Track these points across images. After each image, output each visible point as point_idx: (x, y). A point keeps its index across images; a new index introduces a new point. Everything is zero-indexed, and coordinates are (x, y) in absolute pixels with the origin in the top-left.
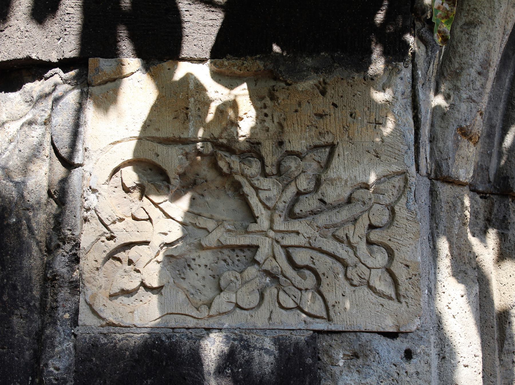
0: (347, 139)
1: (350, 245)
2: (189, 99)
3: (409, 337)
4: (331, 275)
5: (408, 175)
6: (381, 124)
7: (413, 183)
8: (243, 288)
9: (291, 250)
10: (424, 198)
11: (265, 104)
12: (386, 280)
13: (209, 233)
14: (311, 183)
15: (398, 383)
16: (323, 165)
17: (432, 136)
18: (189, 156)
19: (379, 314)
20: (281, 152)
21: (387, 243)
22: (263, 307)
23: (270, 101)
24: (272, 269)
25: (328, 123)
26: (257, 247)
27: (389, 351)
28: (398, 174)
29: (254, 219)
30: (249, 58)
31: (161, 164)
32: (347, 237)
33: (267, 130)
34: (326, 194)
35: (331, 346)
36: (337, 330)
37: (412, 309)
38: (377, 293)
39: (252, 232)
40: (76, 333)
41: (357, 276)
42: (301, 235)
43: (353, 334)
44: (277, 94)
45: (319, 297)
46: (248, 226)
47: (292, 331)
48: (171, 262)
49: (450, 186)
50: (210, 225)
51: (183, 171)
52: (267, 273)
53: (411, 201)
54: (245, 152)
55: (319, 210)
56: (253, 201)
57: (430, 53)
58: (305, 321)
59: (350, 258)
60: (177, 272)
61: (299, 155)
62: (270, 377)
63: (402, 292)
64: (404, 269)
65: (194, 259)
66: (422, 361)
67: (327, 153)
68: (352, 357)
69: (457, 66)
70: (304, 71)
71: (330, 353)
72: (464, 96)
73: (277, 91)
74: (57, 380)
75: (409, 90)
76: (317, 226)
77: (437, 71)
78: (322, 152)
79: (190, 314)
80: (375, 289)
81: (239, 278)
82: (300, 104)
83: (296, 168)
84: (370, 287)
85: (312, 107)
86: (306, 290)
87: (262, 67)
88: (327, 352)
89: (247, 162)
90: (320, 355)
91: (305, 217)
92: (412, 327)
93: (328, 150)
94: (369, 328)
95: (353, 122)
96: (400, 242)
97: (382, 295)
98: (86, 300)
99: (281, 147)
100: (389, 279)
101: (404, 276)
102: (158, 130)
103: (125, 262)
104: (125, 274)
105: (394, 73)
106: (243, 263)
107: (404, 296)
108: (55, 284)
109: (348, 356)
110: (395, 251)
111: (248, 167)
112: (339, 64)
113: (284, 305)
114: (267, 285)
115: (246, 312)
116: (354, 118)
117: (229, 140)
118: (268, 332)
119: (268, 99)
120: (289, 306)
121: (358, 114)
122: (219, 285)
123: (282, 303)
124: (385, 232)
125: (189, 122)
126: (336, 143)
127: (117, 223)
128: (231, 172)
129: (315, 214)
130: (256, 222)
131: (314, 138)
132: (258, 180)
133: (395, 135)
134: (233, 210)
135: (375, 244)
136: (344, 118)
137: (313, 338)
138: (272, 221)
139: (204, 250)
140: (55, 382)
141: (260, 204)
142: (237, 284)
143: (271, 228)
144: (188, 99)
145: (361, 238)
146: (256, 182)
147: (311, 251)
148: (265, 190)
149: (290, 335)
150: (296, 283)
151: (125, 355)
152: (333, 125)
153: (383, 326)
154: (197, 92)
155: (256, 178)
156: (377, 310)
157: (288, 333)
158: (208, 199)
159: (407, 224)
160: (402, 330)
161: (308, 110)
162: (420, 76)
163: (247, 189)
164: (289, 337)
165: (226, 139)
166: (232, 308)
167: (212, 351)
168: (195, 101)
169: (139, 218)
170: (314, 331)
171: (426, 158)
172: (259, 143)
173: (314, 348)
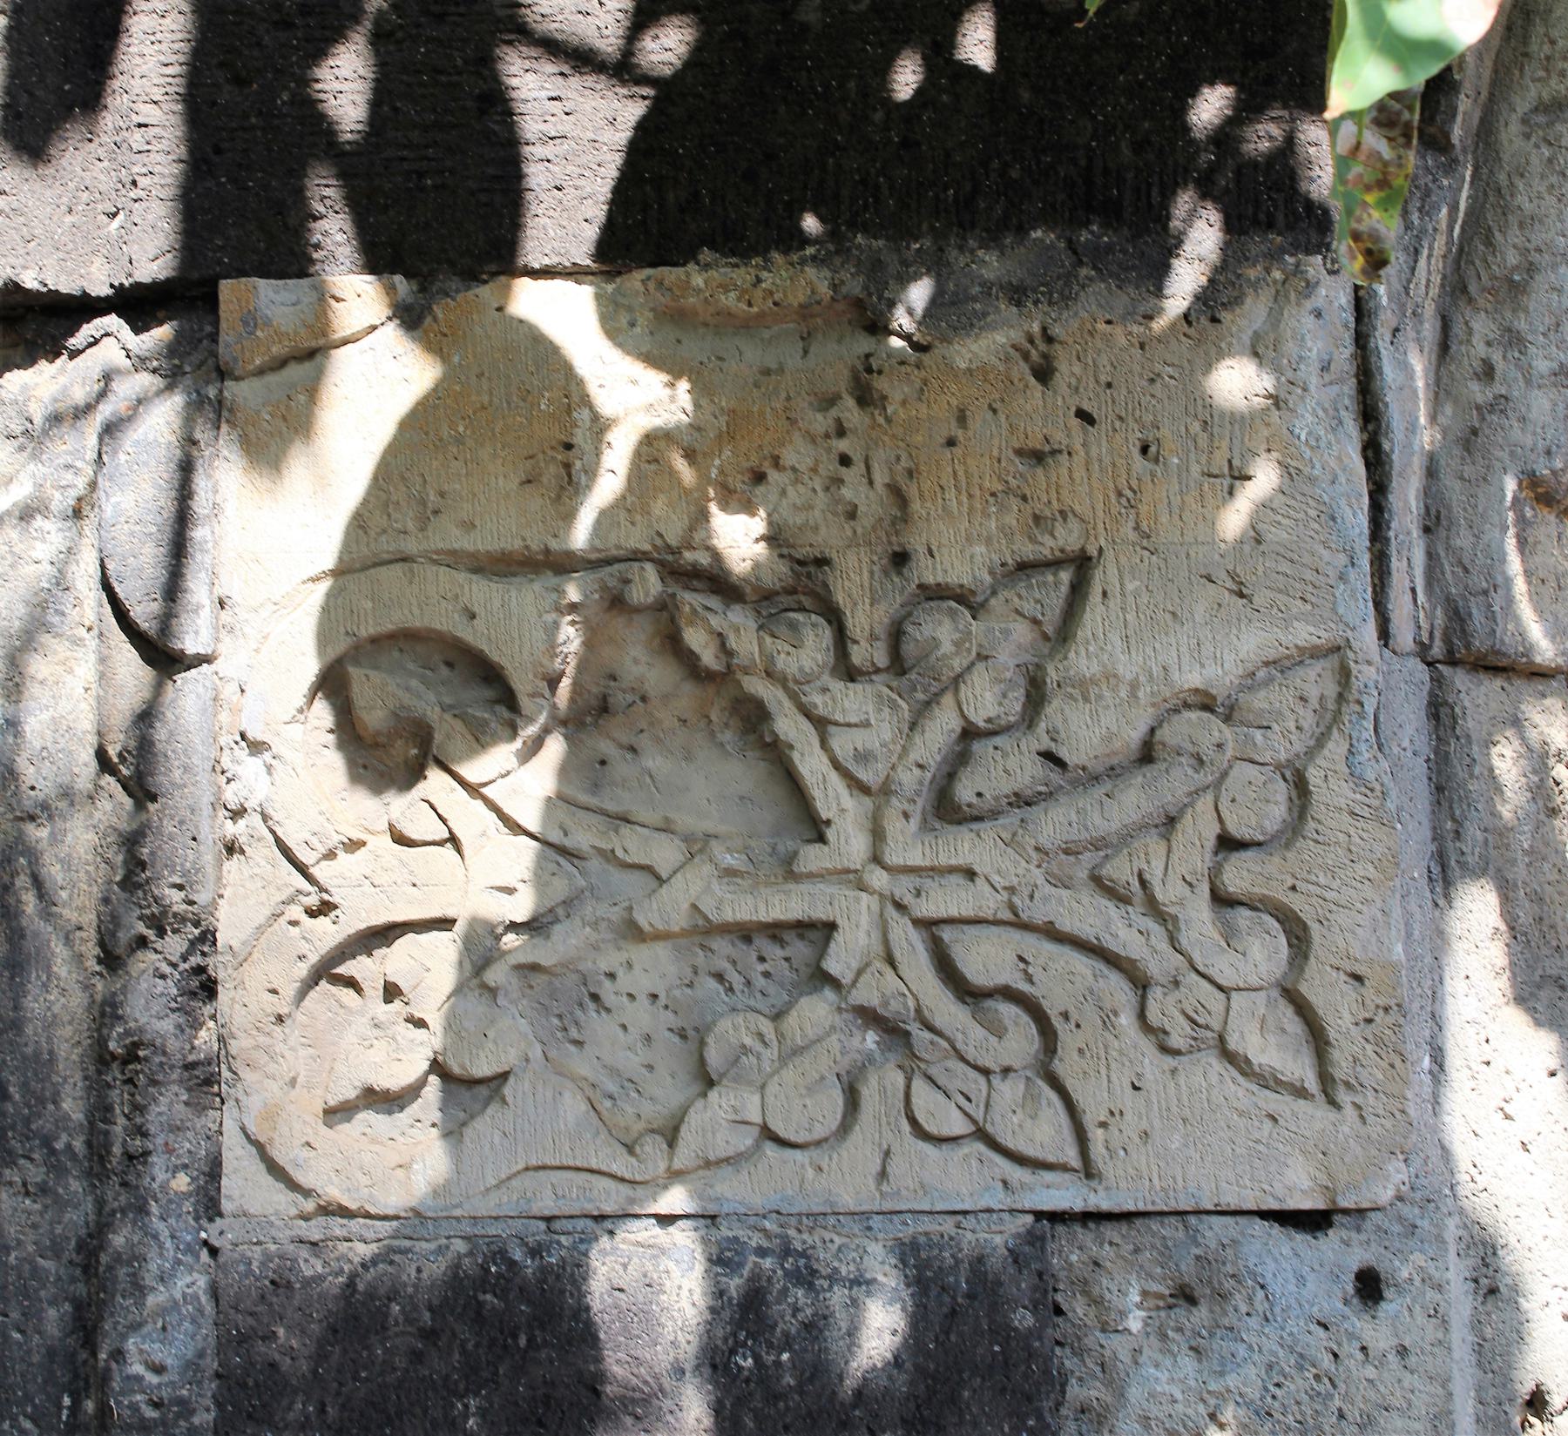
0: (1133, 536)
1: (1154, 908)
2: (575, 414)
3: (1368, 1225)
4: (1091, 1018)
5: (1350, 654)
7: (1371, 684)
8: (784, 1072)
9: (947, 934)
10: (1409, 730)
11: (839, 421)
12: (1283, 1030)
14: (1010, 695)
15: (1334, 1386)
16: (1049, 629)
17: (1433, 512)
19: (1261, 1148)
20: (904, 587)
21: (1285, 900)
22: (856, 1135)
23: (856, 411)
24: (886, 1004)
25: (1061, 482)
26: (831, 927)
27: (1306, 1274)
28: (1316, 653)
29: (817, 829)
30: (777, 257)
31: (485, 648)
32: (1143, 883)
33: (852, 515)
34: (1063, 735)
35: (1096, 1264)
36: (1116, 1209)
37: (1374, 1129)
38: (1255, 1074)
42: (980, 881)
43: (1173, 1219)
44: (881, 384)
45: (1053, 1096)
46: (796, 853)
47: (960, 1218)
48: (531, 987)
49: (1498, 682)
50: (664, 854)
52: (869, 1017)
53: (1363, 747)
55: (1043, 789)
56: (811, 765)
57: (1415, 217)
58: (1005, 1183)
60: (556, 1021)
61: (965, 599)
62: (890, 1377)
63: (1341, 1067)
64: (1345, 987)
65: (611, 976)
66: (1417, 1309)
67: (1064, 589)
69: (1512, 258)
70: (975, 299)
71: (1096, 1291)
72: (1542, 366)
73: (880, 372)
74: (157, 1405)
75: (1345, 353)
76: (1037, 849)
77: (1444, 277)
78: (1045, 583)
79: (604, 1168)
80: (1248, 1061)
81: (770, 1035)
82: (962, 419)
83: (957, 644)
84: (1229, 1056)
85: (1005, 425)
86: (1007, 1071)
87: (824, 289)
88: (1084, 1287)
89: (782, 630)
90: (1059, 1298)
91: (995, 814)
92: (1380, 1191)
93: (1065, 576)
94: (1231, 1200)
95: (1153, 475)
96: (1330, 895)
97: (1272, 1083)
98: (243, 1129)
99: (900, 573)
100: (1294, 1026)
101: (1346, 1015)
102: (469, 526)
103: (374, 991)
104: (377, 1032)
105: (1293, 295)
106: (782, 985)
107: (1347, 1084)
108: (137, 1072)
109: (1160, 1296)
110: (1314, 927)
111: (787, 648)
112: (1095, 268)
113: (932, 1128)
114: (870, 1059)
115: (798, 1155)
116: (1157, 461)
118: (876, 1222)
119: (850, 402)
120: (946, 1132)
121: (1168, 445)
122: (702, 1061)
124: (1276, 859)
126: (1092, 551)
127: (341, 854)
128: (729, 666)
129: (1028, 804)
130: (821, 839)
131: (1018, 537)
132: (825, 690)
133: (1301, 516)
134: (742, 798)
135: (1242, 904)
136: (1121, 462)
137: (1034, 1239)
138: (878, 834)
139: (644, 941)
140: (150, 1413)
141: (834, 776)
142: (764, 1057)
143: (876, 859)
144: (569, 411)
145: (1190, 885)
146: (817, 699)
147: (1016, 935)
148: (849, 725)
149: (953, 1232)
151: (386, 1315)
152: (1083, 489)
153: (1279, 1189)
155: (819, 683)
156: (1257, 1135)
157: (948, 1226)
158: (654, 761)
159: (1352, 831)
161: (990, 439)
162: (1384, 301)
163: (789, 725)
164: (951, 1238)
166: (749, 1142)
167: (685, 1293)
169: (414, 836)
170: (1039, 1215)
171: (1413, 590)
172: (822, 562)
173: (1040, 1275)
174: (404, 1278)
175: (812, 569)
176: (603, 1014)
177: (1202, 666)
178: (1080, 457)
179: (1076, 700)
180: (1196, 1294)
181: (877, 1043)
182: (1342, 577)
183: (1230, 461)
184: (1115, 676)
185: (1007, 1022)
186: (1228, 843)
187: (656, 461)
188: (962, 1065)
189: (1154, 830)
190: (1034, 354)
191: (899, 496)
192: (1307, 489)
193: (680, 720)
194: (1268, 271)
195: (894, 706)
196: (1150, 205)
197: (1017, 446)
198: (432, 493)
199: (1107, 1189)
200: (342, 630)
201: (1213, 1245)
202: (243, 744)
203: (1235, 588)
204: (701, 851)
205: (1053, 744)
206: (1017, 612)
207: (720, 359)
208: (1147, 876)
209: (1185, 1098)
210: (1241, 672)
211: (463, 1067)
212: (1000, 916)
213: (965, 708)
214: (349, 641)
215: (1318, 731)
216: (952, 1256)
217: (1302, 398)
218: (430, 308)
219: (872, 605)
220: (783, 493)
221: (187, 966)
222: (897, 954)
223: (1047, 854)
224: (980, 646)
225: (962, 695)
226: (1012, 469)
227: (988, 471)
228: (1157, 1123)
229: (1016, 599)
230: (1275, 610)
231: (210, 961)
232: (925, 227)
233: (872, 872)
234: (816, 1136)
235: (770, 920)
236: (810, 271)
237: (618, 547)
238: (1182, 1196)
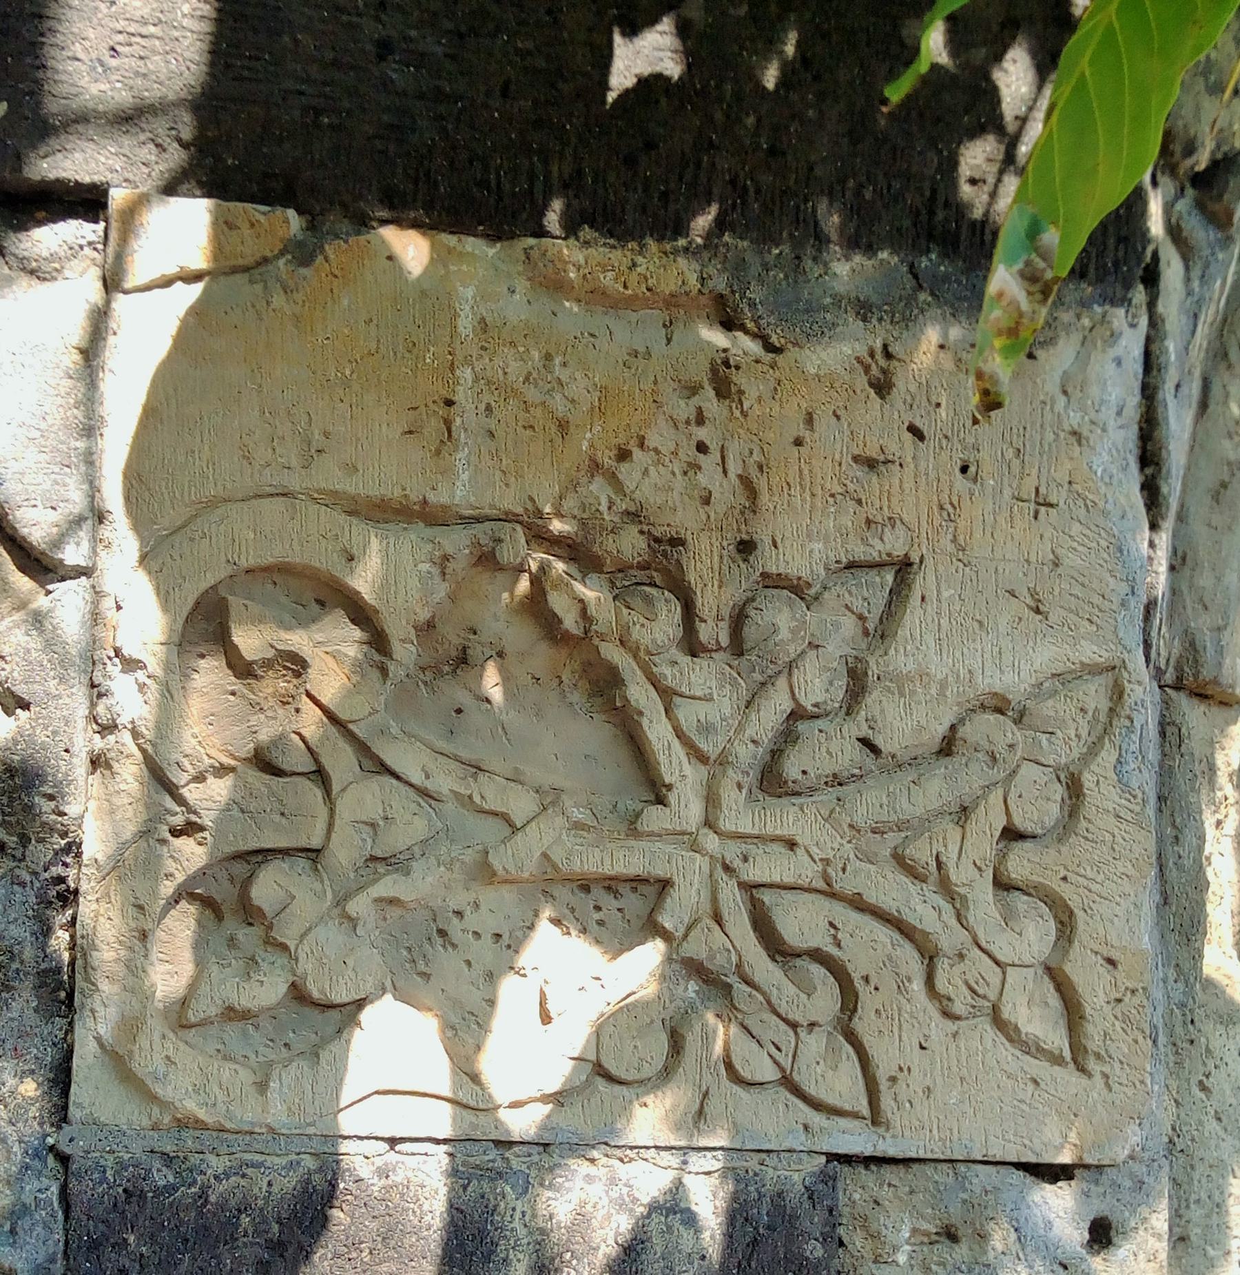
0: (950, 548)
1: (946, 887)
2: (458, 372)
4: (888, 982)
5: (1126, 675)
6: (1051, 505)
9: (767, 897)
11: (700, 411)
13: (515, 829)
14: (835, 682)
16: (871, 626)
18: (451, 566)
19: (1024, 1107)
21: (1057, 889)
23: (715, 400)
24: (712, 957)
26: (664, 885)
28: (1094, 670)
29: (658, 793)
33: (707, 501)
34: (880, 724)
36: (901, 1155)
39: (651, 834)
40: (68, 1151)
41: (964, 989)
42: (800, 851)
43: (945, 1166)
44: (739, 379)
46: (638, 815)
47: (764, 1156)
51: (428, 616)
52: (696, 969)
53: (1130, 758)
54: (631, 567)
55: (856, 771)
56: (657, 731)
57: (1196, 284)
58: (806, 1127)
59: (948, 936)
61: (797, 588)
63: (1094, 1041)
64: (1102, 970)
65: (459, 914)
66: (1141, 1256)
68: (935, 1238)
70: (826, 309)
71: (874, 1227)
73: (737, 368)
75: (1134, 401)
76: (851, 826)
82: (810, 420)
85: (847, 433)
88: (864, 1222)
89: (637, 602)
90: (841, 1231)
91: (812, 790)
92: (1119, 1150)
94: (997, 1153)
97: (1033, 1050)
100: (1054, 1000)
101: (1101, 993)
102: (351, 469)
105: (1099, 343)
107: (1098, 1056)
110: (1079, 913)
111: (642, 620)
112: (932, 294)
113: (746, 1074)
116: (975, 480)
117: (583, 523)
119: (711, 393)
120: (759, 1078)
121: (987, 468)
123: (738, 1067)
124: (1052, 852)
126: (915, 558)
127: (211, 780)
129: (840, 784)
130: (661, 801)
133: (1094, 545)
136: (944, 477)
137: (827, 1178)
138: (712, 800)
141: (676, 743)
143: (709, 823)
144: (452, 368)
145: (980, 869)
146: (667, 671)
149: (757, 1168)
150: (784, 1003)
152: (911, 500)
153: (1038, 1147)
154: (483, 348)
156: (1021, 1096)
159: (1116, 831)
160: (1089, 1160)
161: (832, 442)
162: (1173, 358)
163: (639, 693)
164: (756, 1174)
165: (575, 517)
167: (518, 1215)
168: (476, 379)
169: (285, 767)
170: (832, 1157)
172: (677, 542)
173: (831, 1211)
174: (256, 1190)
175: (668, 548)
176: (450, 949)
177: (1002, 672)
178: (910, 469)
179: (893, 694)
180: (960, 1234)
182: (1123, 604)
183: (1037, 490)
184: (927, 674)
185: (816, 981)
186: (1011, 834)
187: (532, 427)
188: (775, 1017)
189: (948, 817)
190: (875, 371)
191: (746, 483)
192: (1101, 521)
193: (533, 678)
194: (1078, 317)
195: (734, 684)
196: (983, 242)
197: (856, 452)
198: (316, 432)
199: (893, 1136)
200: (223, 559)
202: (117, 660)
203: (1033, 604)
204: (553, 803)
205: (870, 732)
206: (847, 606)
207: (592, 335)
208: (944, 859)
209: (964, 1058)
211: (322, 992)
213: (797, 691)
214: (229, 570)
215: (1090, 740)
216: (757, 1190)
217: (1101, 438)
218: (322, 247)
219: (720, 587)
220: (646, 472)
221: (47, 875)
222: (726, 916)
223: (859, 831)
224: (812, 635)
227: (830, 474)
228: (939, 1080)
229: (847, 595)
230: (1066, 628)
231: (72, 873)
232: (785, 234)
233: (706, 835)
235: (613, 873)
236: (682, 262)
237: (492, 506)
238: (956, 1146)
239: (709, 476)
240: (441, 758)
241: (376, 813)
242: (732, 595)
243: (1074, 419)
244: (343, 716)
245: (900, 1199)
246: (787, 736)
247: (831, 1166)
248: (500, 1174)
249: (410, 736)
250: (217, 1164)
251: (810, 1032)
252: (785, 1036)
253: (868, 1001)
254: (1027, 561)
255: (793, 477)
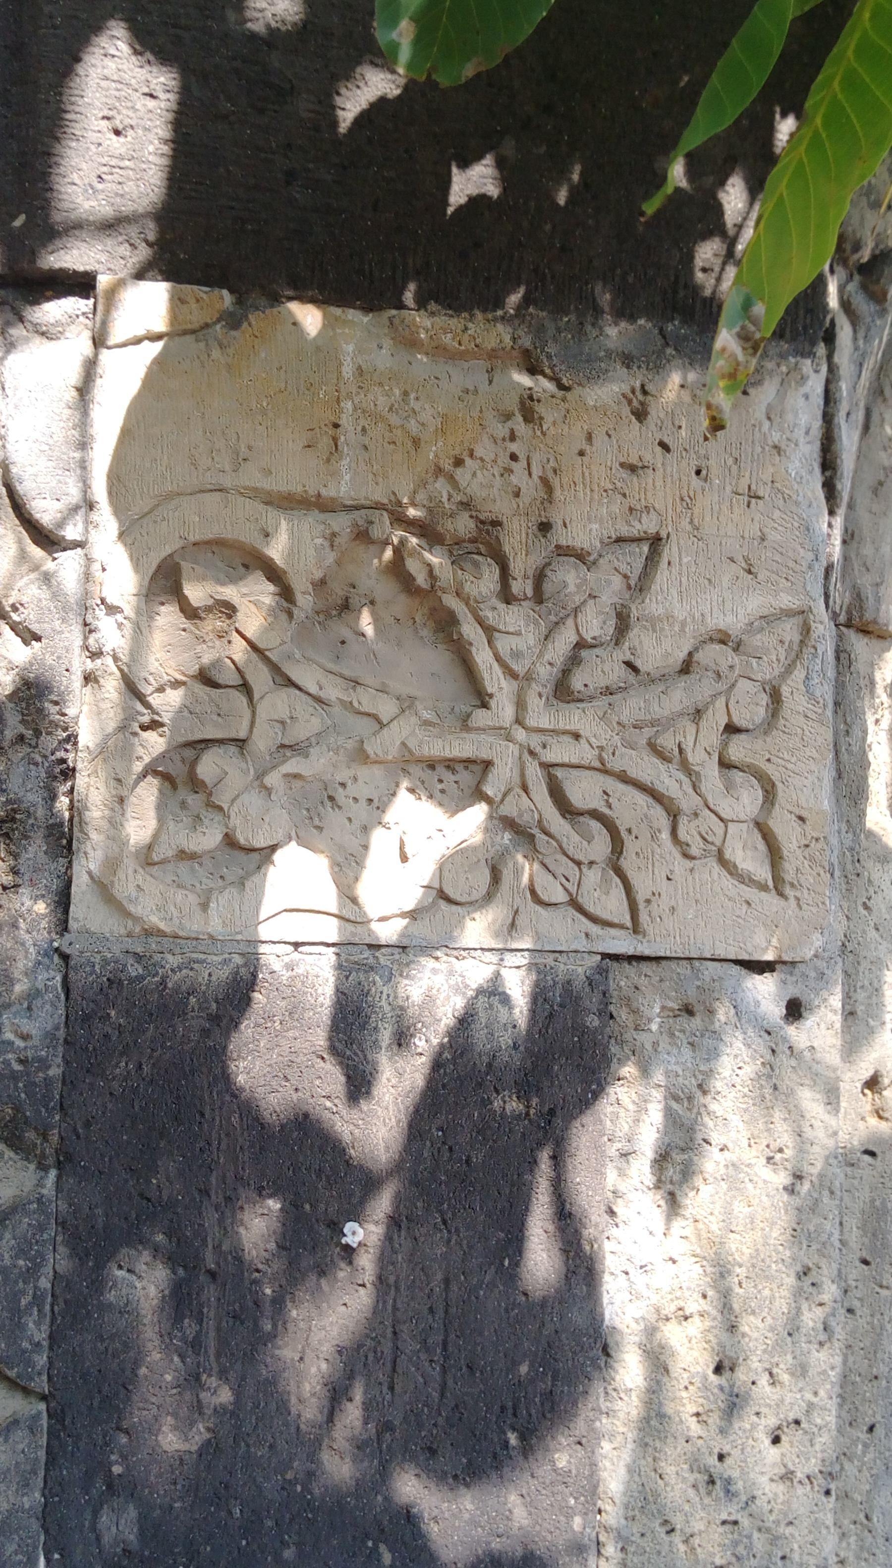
0: (689, 528)
1: (685, 766)
2: (342, 404)
4: (645, 835)
5: (812, 617)
6: (759, 498)
9: (559, 773)
13: (382, 725)
15: (773, 1070)
16: (632, 583)
18: (337, 541)
19: (740, 920)
23: (523, 424)
24: (521, 815)
26: (487, 764)
28: (789, 613)
29: (483, 700)
30: (479, 315)
32: (681, 751)
33: (517, 495)
36: (653, 955)
39: (478, 729)
40: (68, 951)
42: (583, 741)
43: (685, 962)
44: (540, 409)
46: (469, 715)
47: (557, 955)
52: (509, 824)
53: (815, 675)
54: (464, 541)
55: (622, 685)
56: (482, 657)
57: (861, 342)
58: (587, 935)
59: (687, 800)
61: (581, 556)
62: (510, 1056)
63: (789, 874)
64: (795, 824)
65: (343, 785)
66: (823, 1026)
68: (677, 1013)
70: (601, 360)
71: (635, 1005)
73: (539, 401)
74: (20, 1061)
75: (817, 424)
76: (619, 723)
80: (735, 866)
82: (589, 438)
83: (578, 586)
84: (722, 861)
85: (616, 447)
86: (591, 863)
87: (507, 339)
88: (627, 1002)
89: (468, 566)
90: (612, 1008)
91: (591, 698)
96: (790, 766)
97: (747, 880)
99: (544, 536)
100: (761, 846)
101: (794, 842)
102: (267, 472)
105: (793, 384)
107: (792, 885)
108: (13, 830)
109: (672, 1010)
110: (779, 785)
111: (472, 578)
112: (676, 349)
113: (545, 897)
114: (507, 849)
116: (706, 480)
117: (430, 510)
119: (521, 419)
120: (553, 900)
121: (714, 471)
123: (539, 893)
124: (760, 741)
125: (341, 459)
126: (664, 534)
127: (168, 690)
130: (485, 705)
131: (619, 520)
135: (736, 768)
136: (684, 478)
137: (602, 971)
138: (520, 705)
140: (17, 1067)
141: (496, 665)
143: (519, 721)
144: (338, 401)
145: (709, 754)
146: (490, 614)
149: (553, 964)
150: (571, 848)
151: (187, 1004)
153: (750, 948)
154: (360, 387)
156: (738, 913)
159: (805, 727)
160: (785, 958)
161: (605, 455)
162: (845, 394)
163: (470, 630)
164: (552, 968)
167: (384, 996)
168: (355, 409)
169: (221, 681)
170: (605, 956)
172: (496, 523)
173: (604, 994)
174: (200, 979)
177: (725, 615)
178: (660, 473)
180: (695, 1009)
181: (510, 840)
182: (810, 567)
185: (594, 832)
186: (731, 729)
187: (394, 443)
190: (635, 403)
191: (545, 482)
192: (794, 509)
194: (778, 365)
195: (536, 623)
196: (711, 313)
197: (622, 460)
198: (243, 446)
199: (648, 941)
200: (177, 535)
201: (708, 979)
202: (102, 607)
203: (746, 567)
204: (409, 707)
206: (616, 569)
207: (437, 378)
208: (684, 746)
209: (698, 887)
210: (747, 621)
211: (247, 840)
212: (593, 764)
214: (181, 543)
215: (787, 663)
217: (794, 450)
218: (247, 316)
220: (474, 474)
221: (53, 758)
222: (530, 786)
225: (579, 620)
226: (619, 476)
227: (604, 476)
228: (680, 902)
231: (71, 756)
232: (572, 307)
234: (473, 898)
235: (451, 756)
236: (500, 327)
237: (366, 498)
239: (520, 477)
240: (330, 676)
241: (284, 714)
242: (535, 561)
243: (775, 437)
244: (261, 645)
245: (653, 986)
246: (574, 660)
247: (604, 962)
248: (372, 968)
249: (309, 660)
250: (173, 961)
251: (590, 868)
252: (573, 871)
253: (631, 846)
254: (742, 537)
255: (578, 478)
